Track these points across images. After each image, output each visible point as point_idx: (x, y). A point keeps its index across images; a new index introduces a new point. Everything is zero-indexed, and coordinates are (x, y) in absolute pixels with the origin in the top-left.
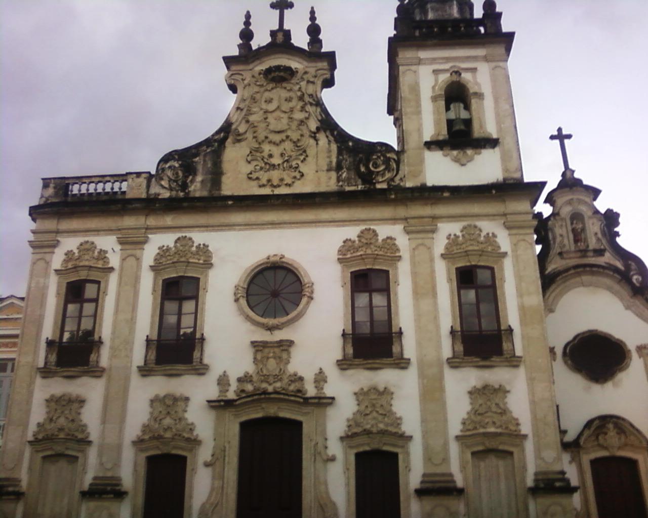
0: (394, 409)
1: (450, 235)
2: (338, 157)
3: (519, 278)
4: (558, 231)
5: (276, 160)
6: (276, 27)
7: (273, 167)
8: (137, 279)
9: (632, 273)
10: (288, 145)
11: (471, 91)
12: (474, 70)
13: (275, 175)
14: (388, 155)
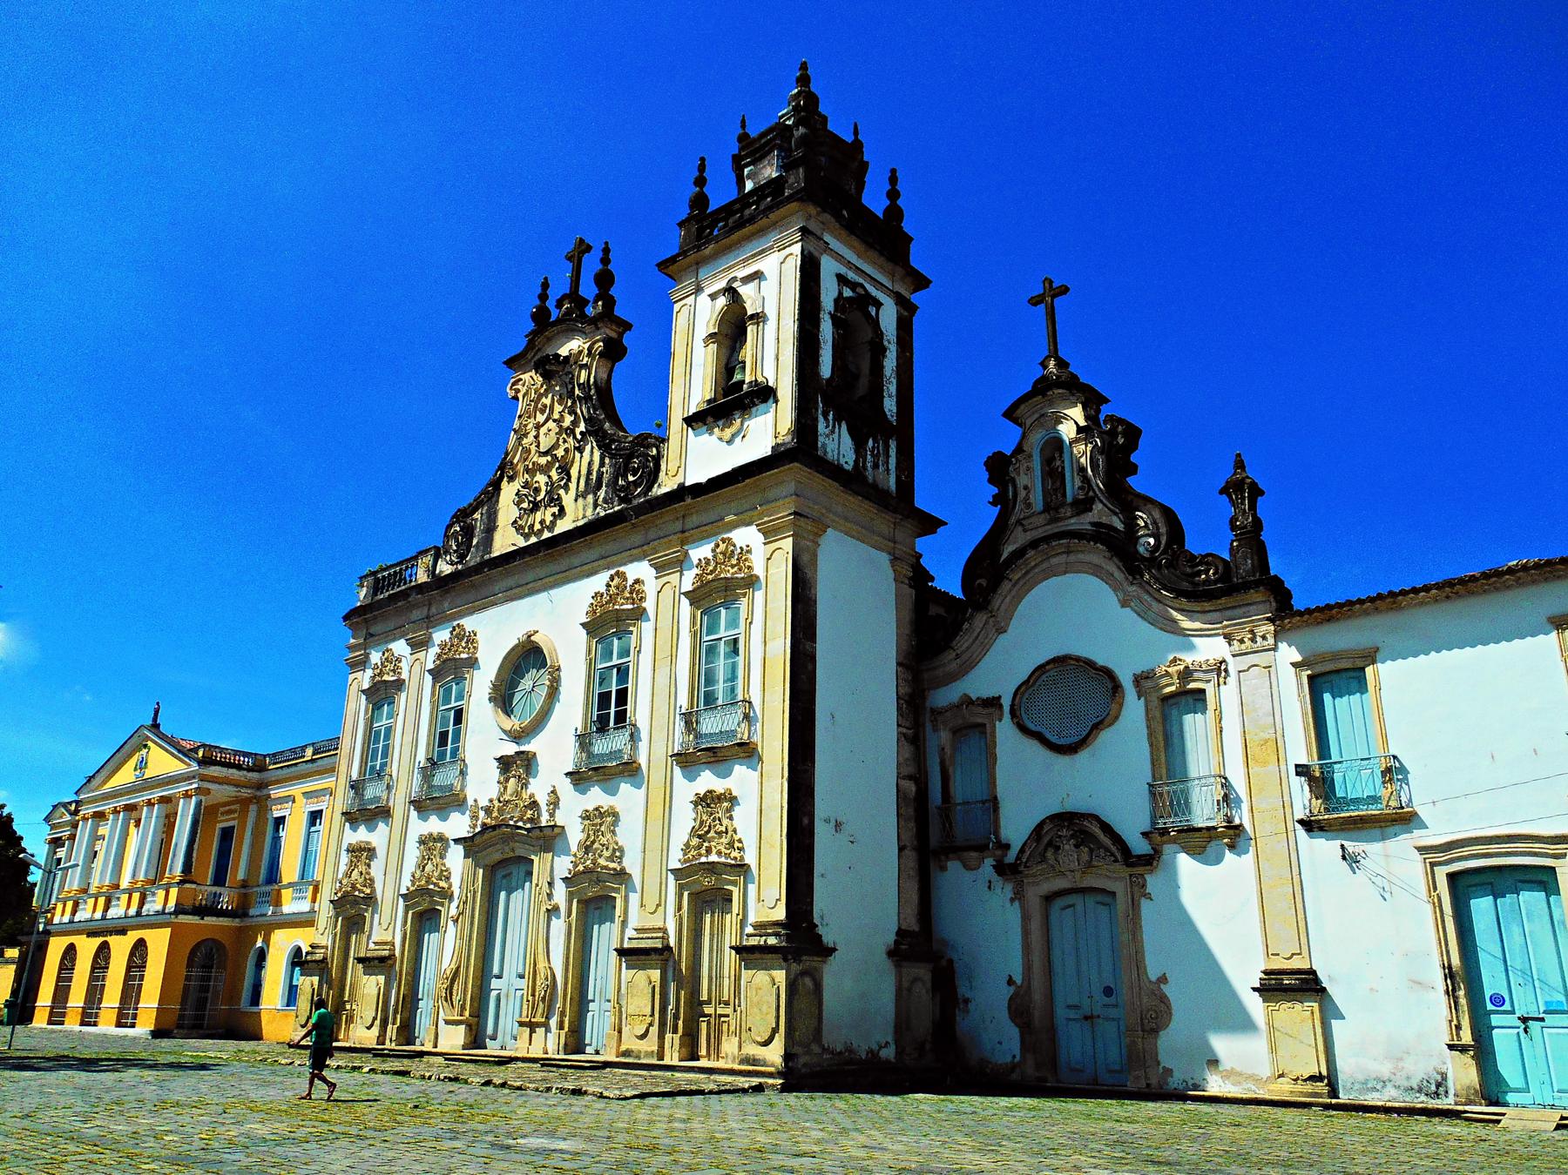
4: (1022, 480)
7: (535, 507)
12: (757, 276)
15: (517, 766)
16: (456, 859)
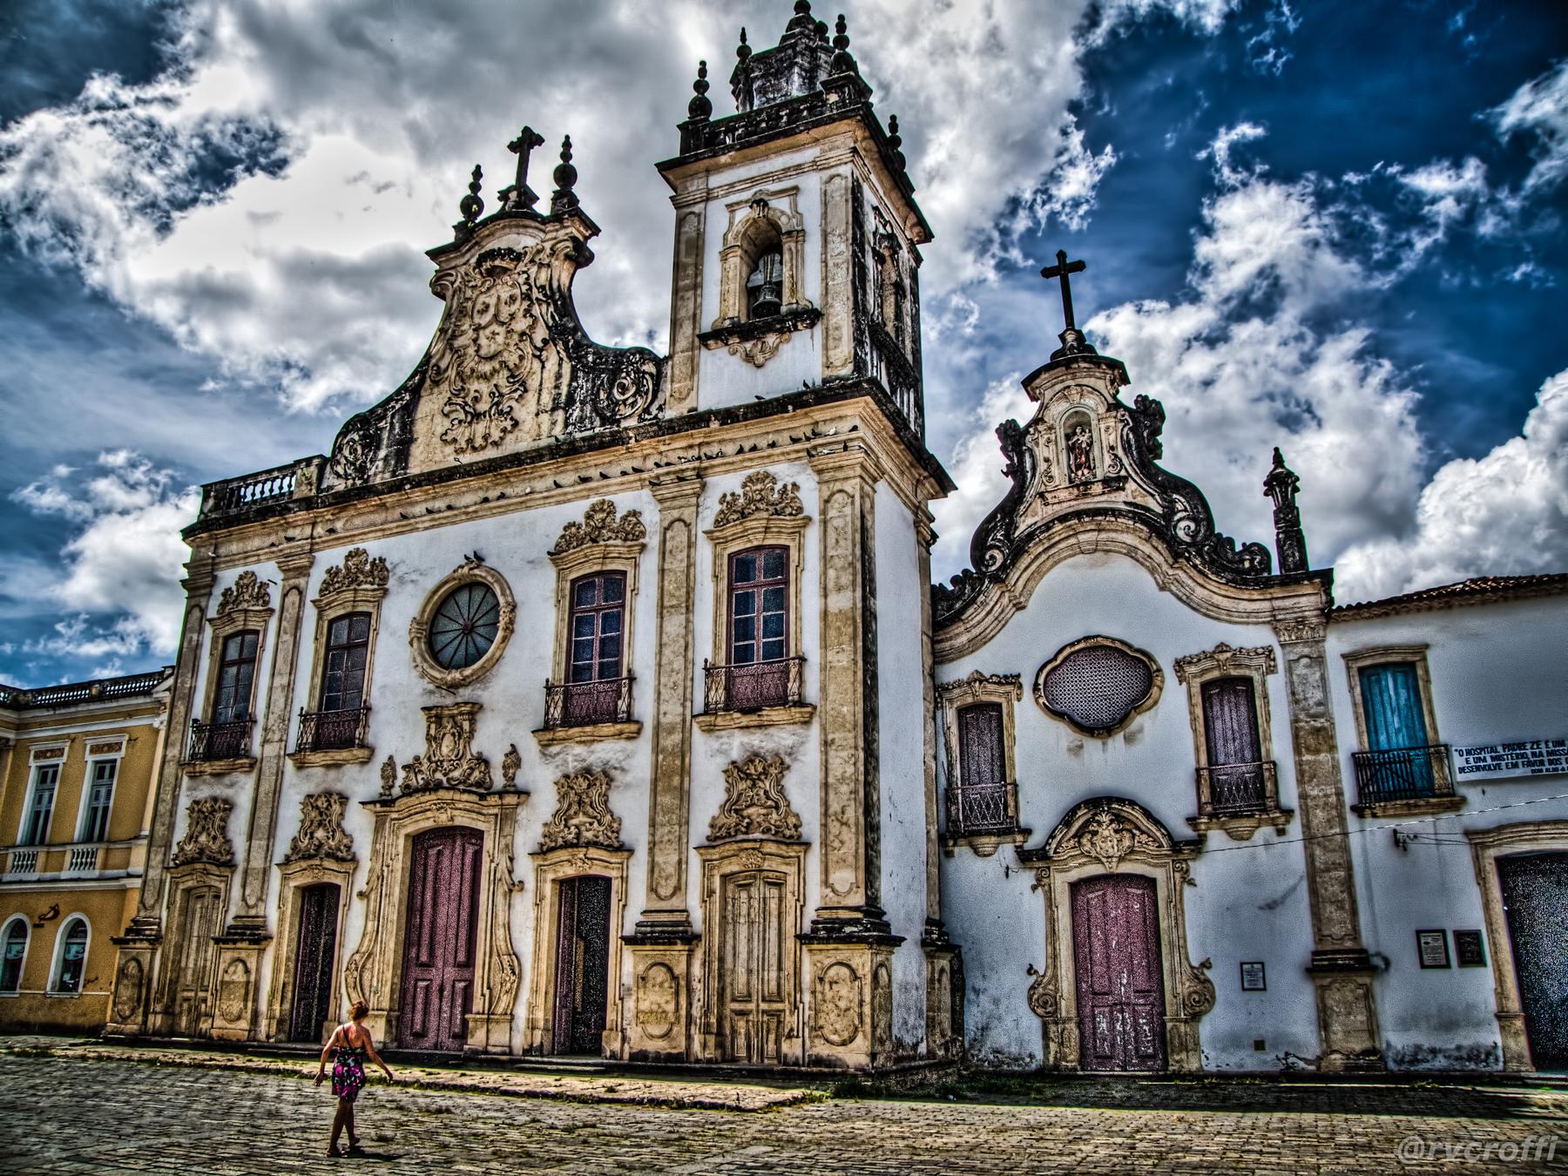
1: (725, 496)
3: (826, 560)
4: (1042, 452)
7: (477, 416)
8: (298, 621)
9: (1179, 515)
10: (501, 379)
13: (480, 428)
15: (451, 718)
16: (358, 822)
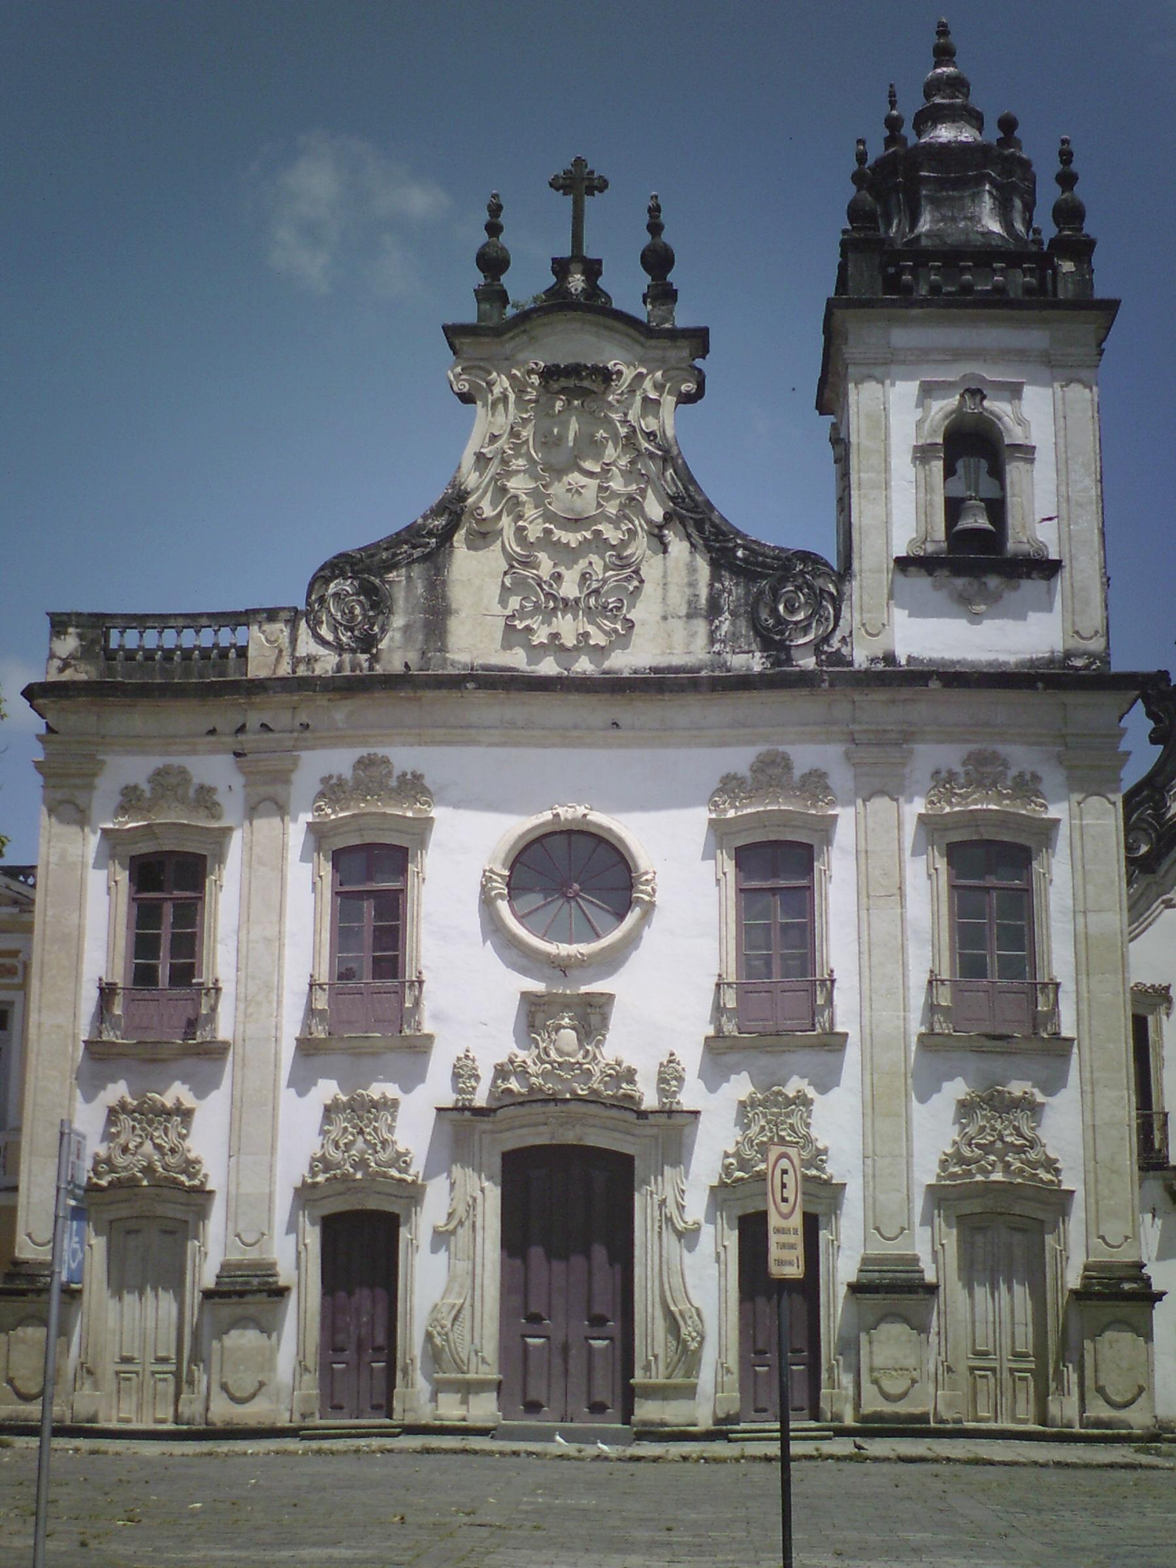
0: (814, 1133)
2: (711, 586)
5: (569, 589)
6: (567, 252)
11: (1007, 441)
14: (819, 583)
